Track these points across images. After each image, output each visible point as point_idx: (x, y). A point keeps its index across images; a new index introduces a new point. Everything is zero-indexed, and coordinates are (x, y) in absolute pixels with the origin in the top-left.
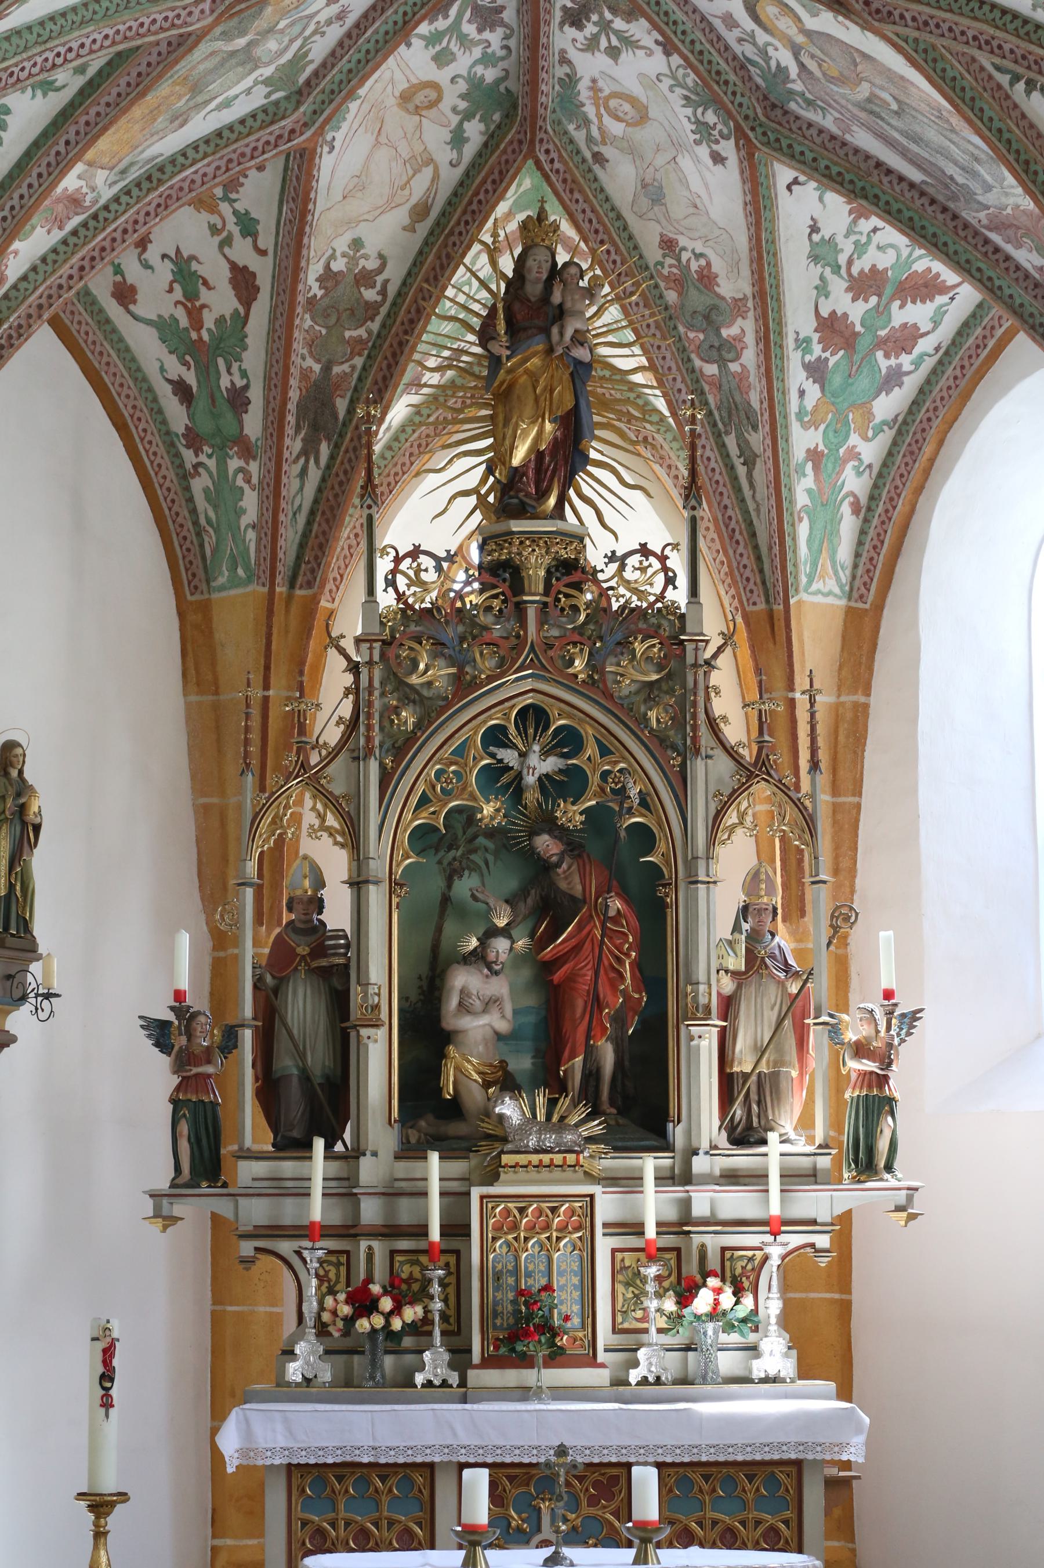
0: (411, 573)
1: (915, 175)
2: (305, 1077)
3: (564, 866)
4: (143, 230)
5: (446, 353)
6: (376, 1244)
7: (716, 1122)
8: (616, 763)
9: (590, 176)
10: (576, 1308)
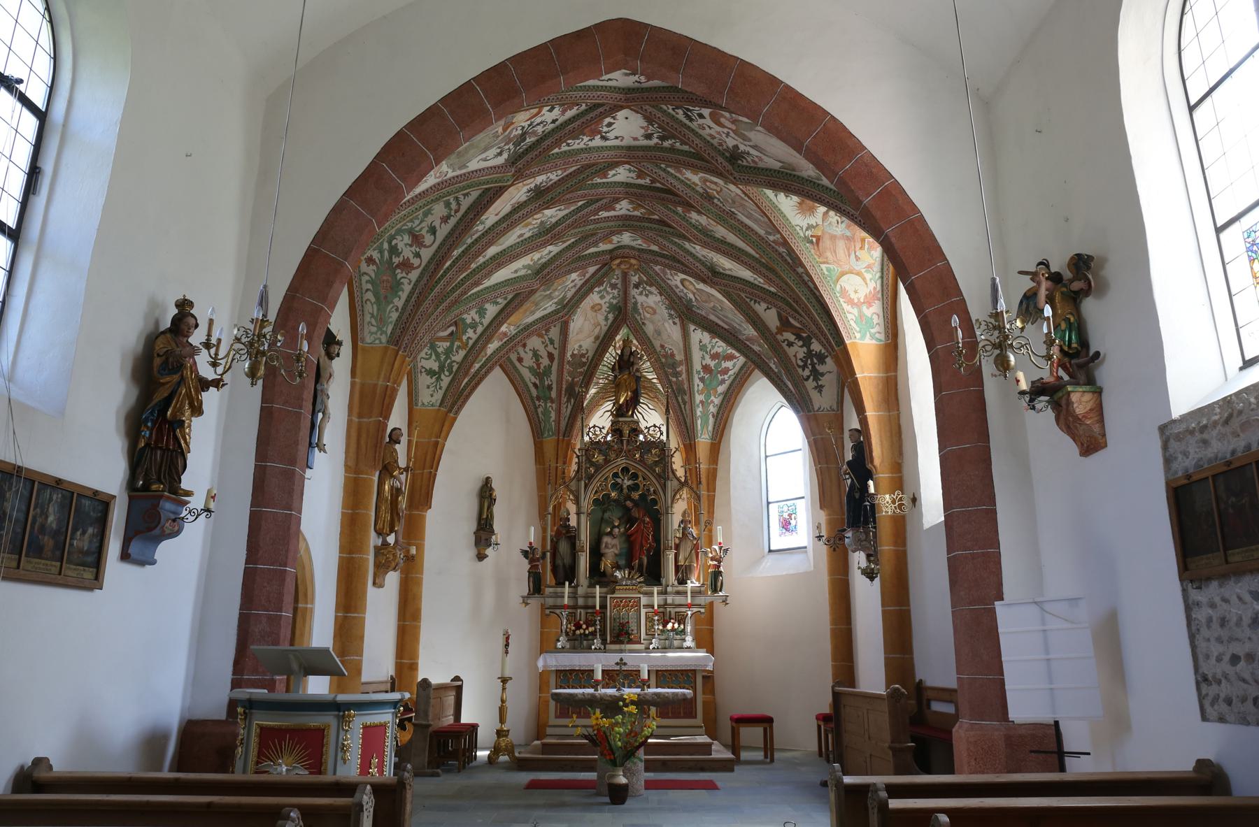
1: (726, 327)
2: (564, 565)
4: (523, 342)
6: (582, 610)
7: (674, 578)
10: (636, 628)
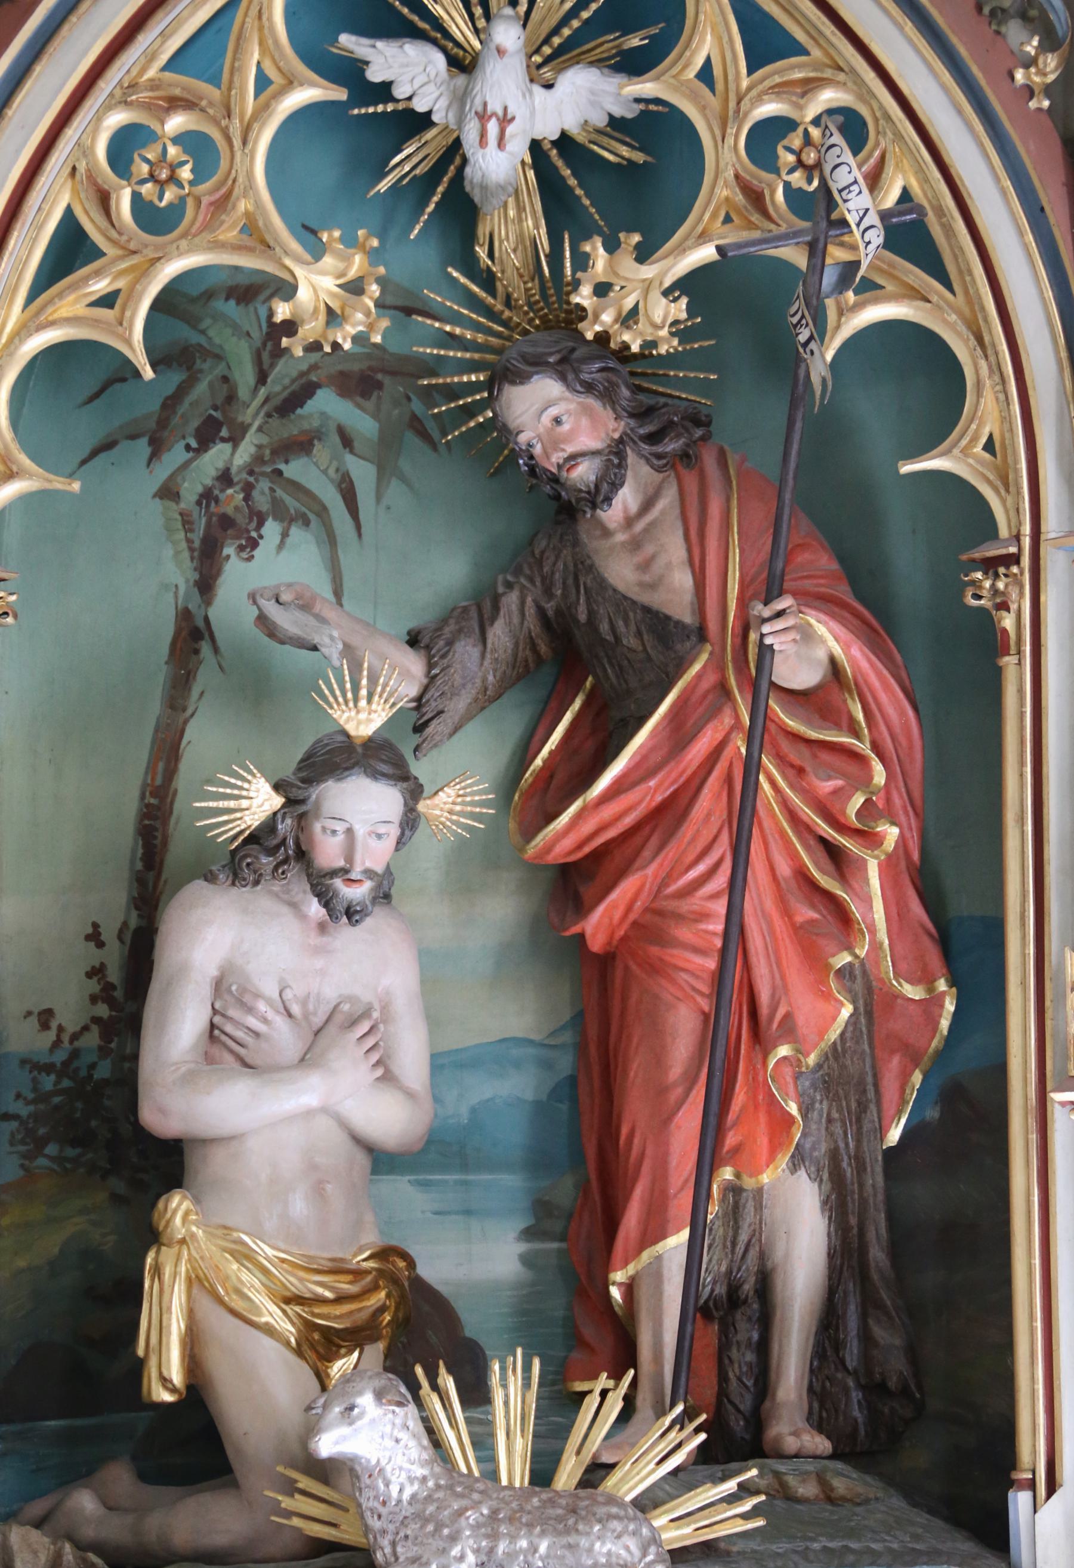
3: (627, 498)
8: (809, 86)
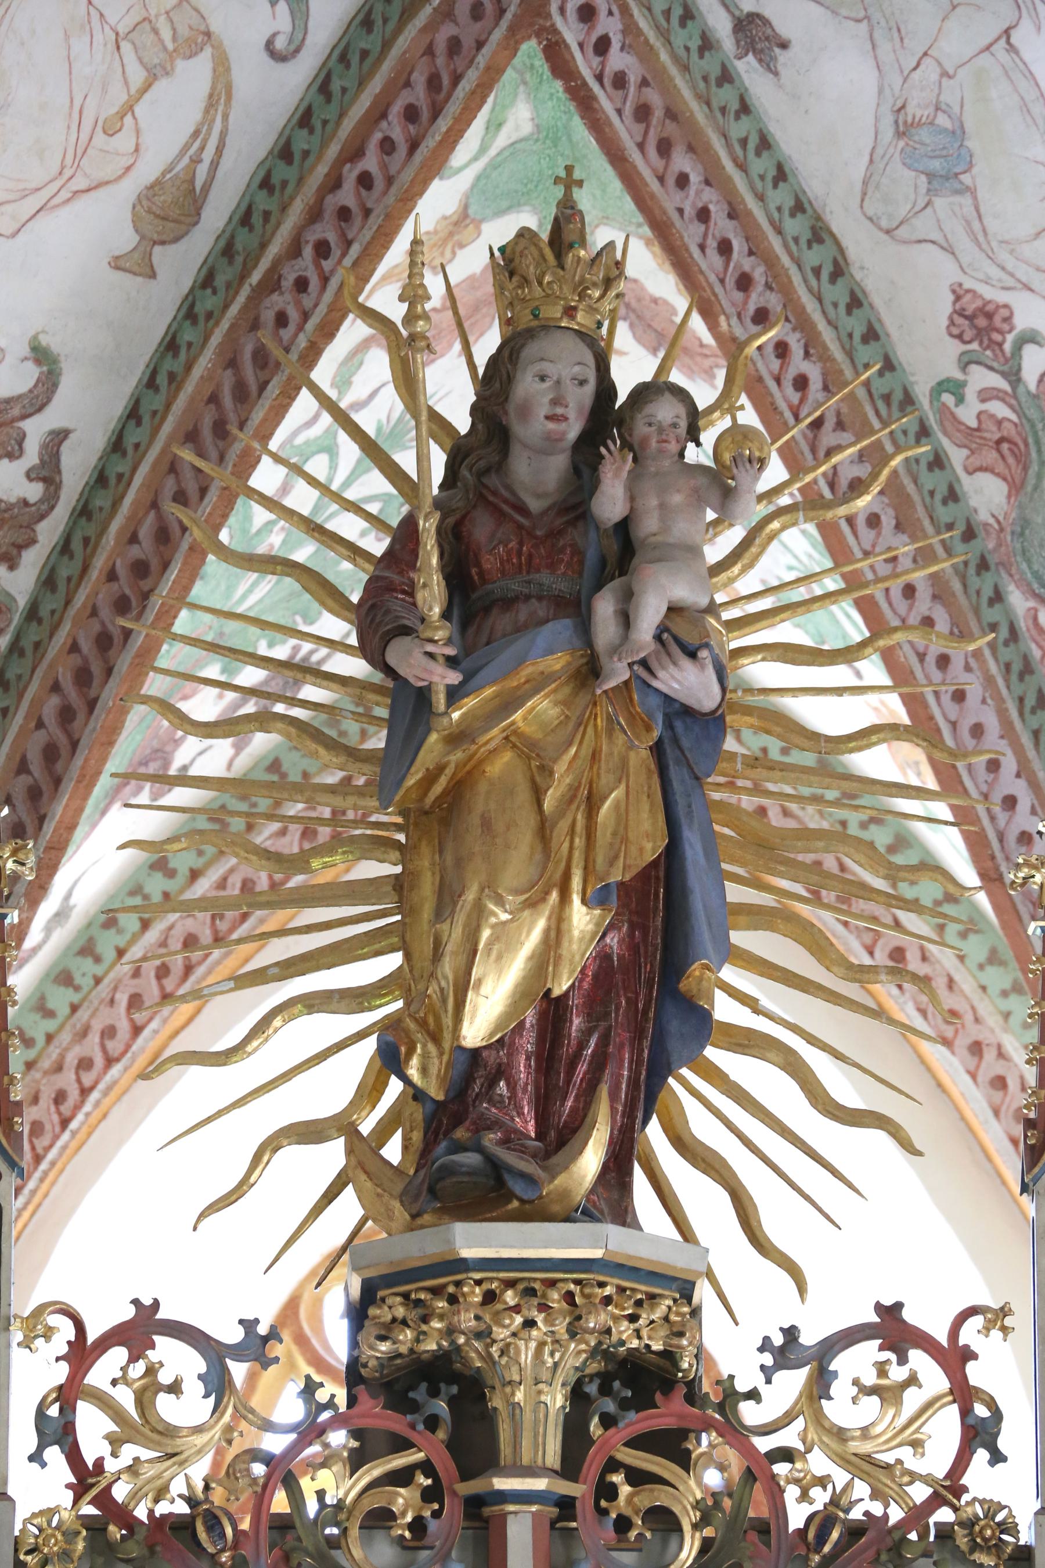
0: (124, 1396)
5: (251, 676)
9: (726, 95)
